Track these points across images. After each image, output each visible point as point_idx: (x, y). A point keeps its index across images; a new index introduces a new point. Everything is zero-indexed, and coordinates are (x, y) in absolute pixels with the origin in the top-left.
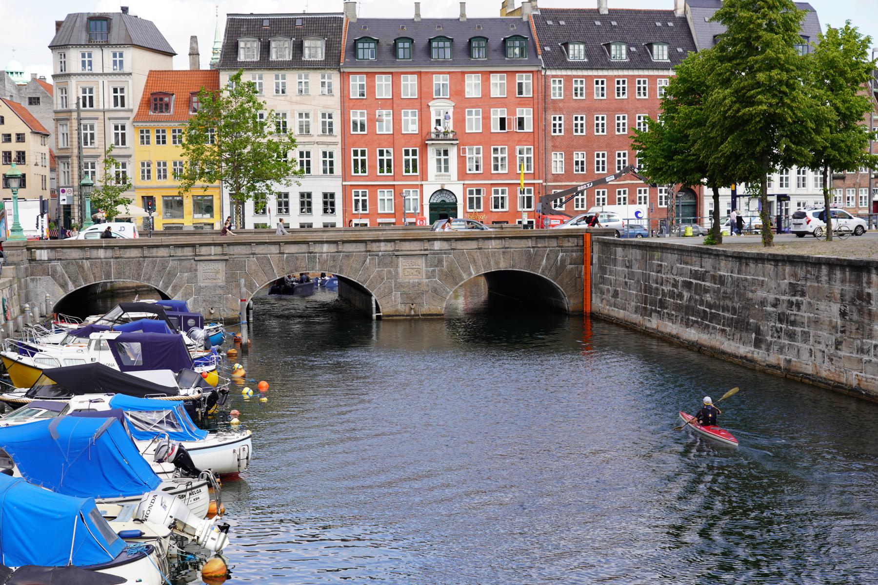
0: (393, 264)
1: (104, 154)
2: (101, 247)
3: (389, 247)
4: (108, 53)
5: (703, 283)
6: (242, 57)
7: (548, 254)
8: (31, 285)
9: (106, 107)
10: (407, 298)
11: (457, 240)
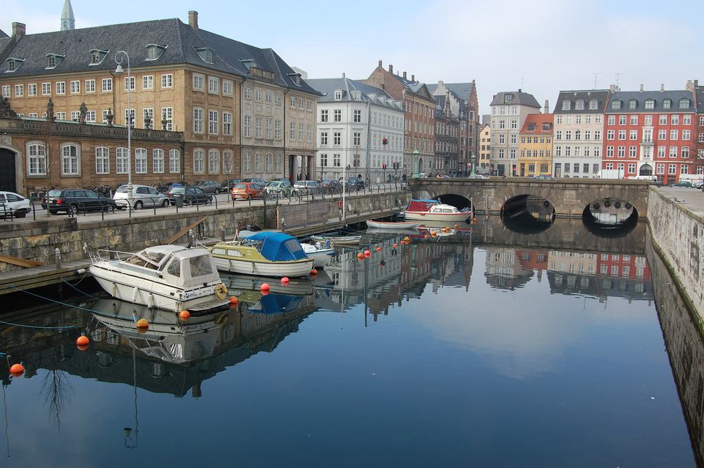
4: (511, 107)
6: (564, 109)
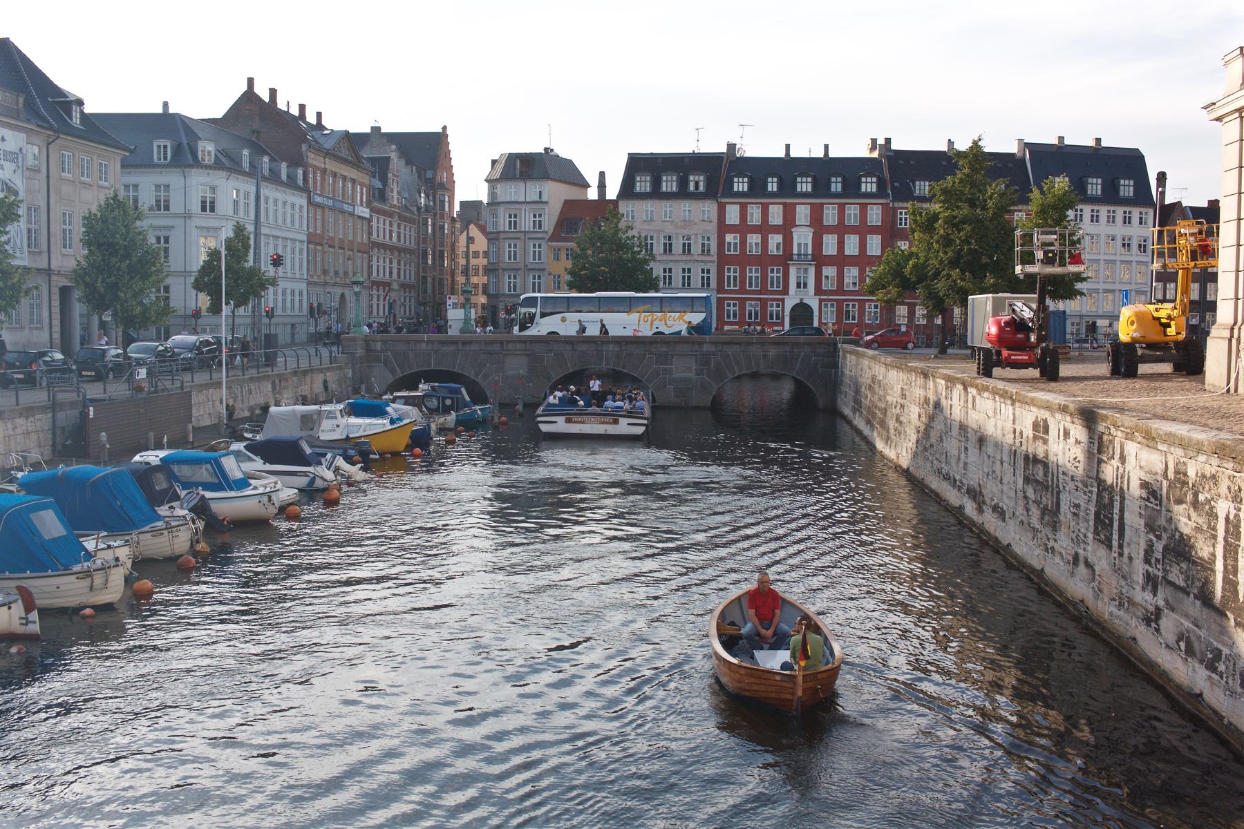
3: (664, 349)
11: (723, 343)
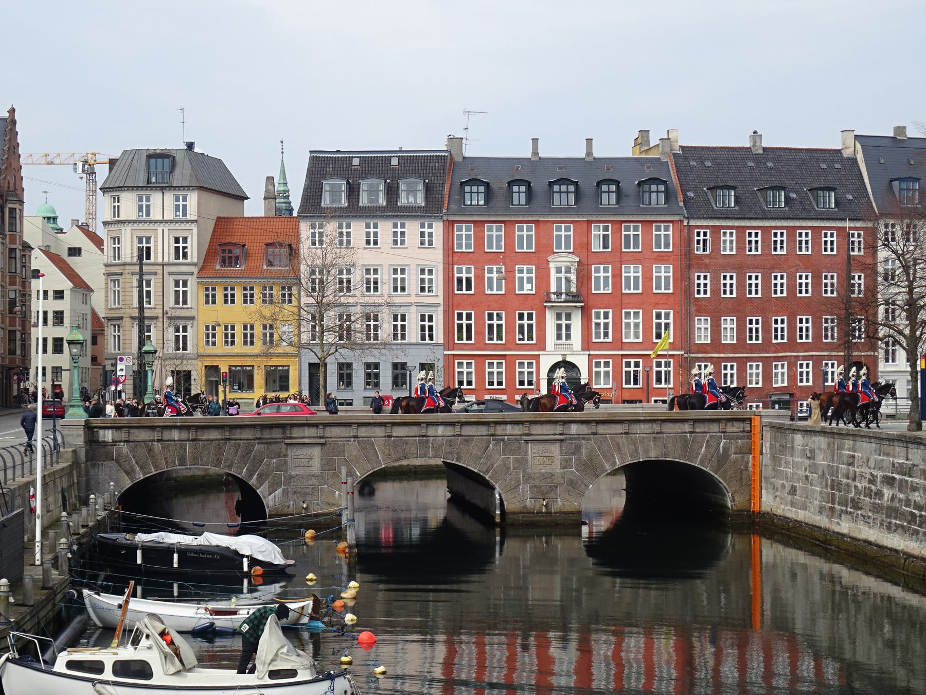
0: (521, 451)
1: (161, 315)
2: (175, 427)
3: (517, 430)
4: (169, 197)
5: (910, 479)
6: (326, 201)
7: (708, 441)
8: (92, 472)
9: (166, 260)
10: (537, 492)
11: (598, 422)
